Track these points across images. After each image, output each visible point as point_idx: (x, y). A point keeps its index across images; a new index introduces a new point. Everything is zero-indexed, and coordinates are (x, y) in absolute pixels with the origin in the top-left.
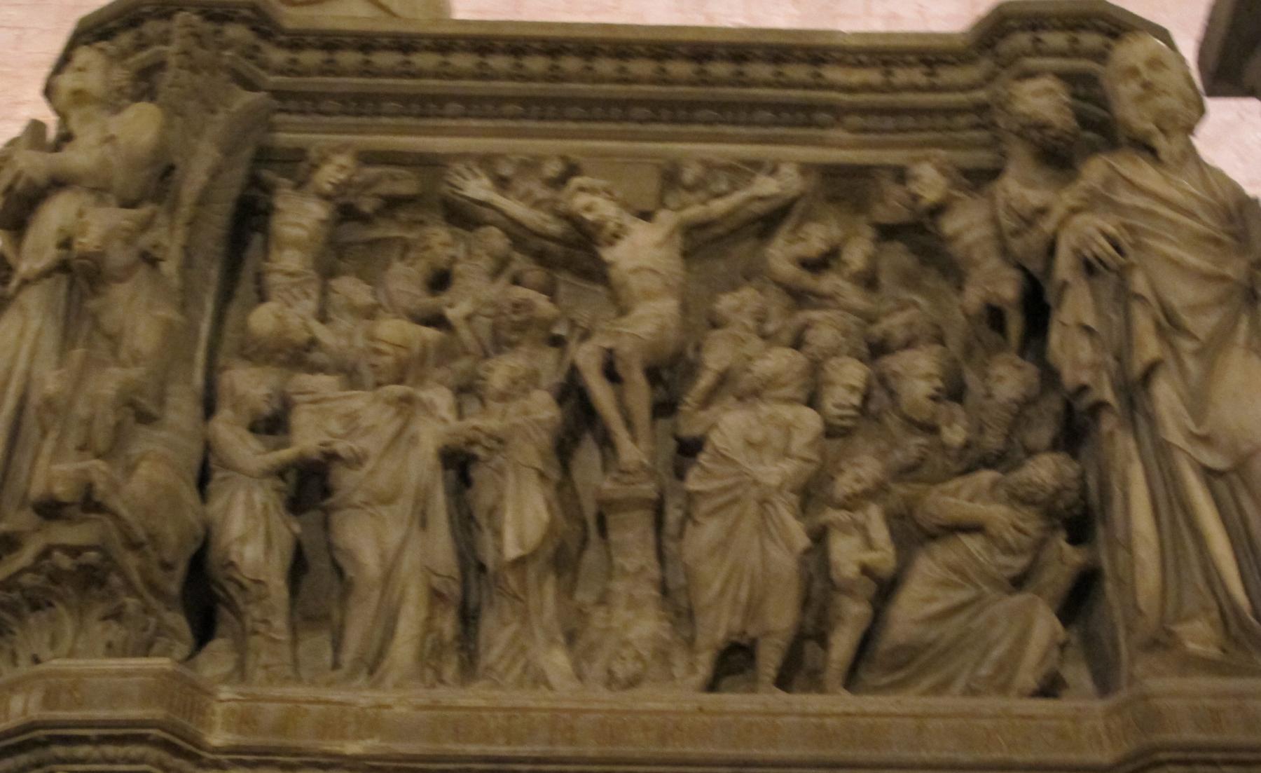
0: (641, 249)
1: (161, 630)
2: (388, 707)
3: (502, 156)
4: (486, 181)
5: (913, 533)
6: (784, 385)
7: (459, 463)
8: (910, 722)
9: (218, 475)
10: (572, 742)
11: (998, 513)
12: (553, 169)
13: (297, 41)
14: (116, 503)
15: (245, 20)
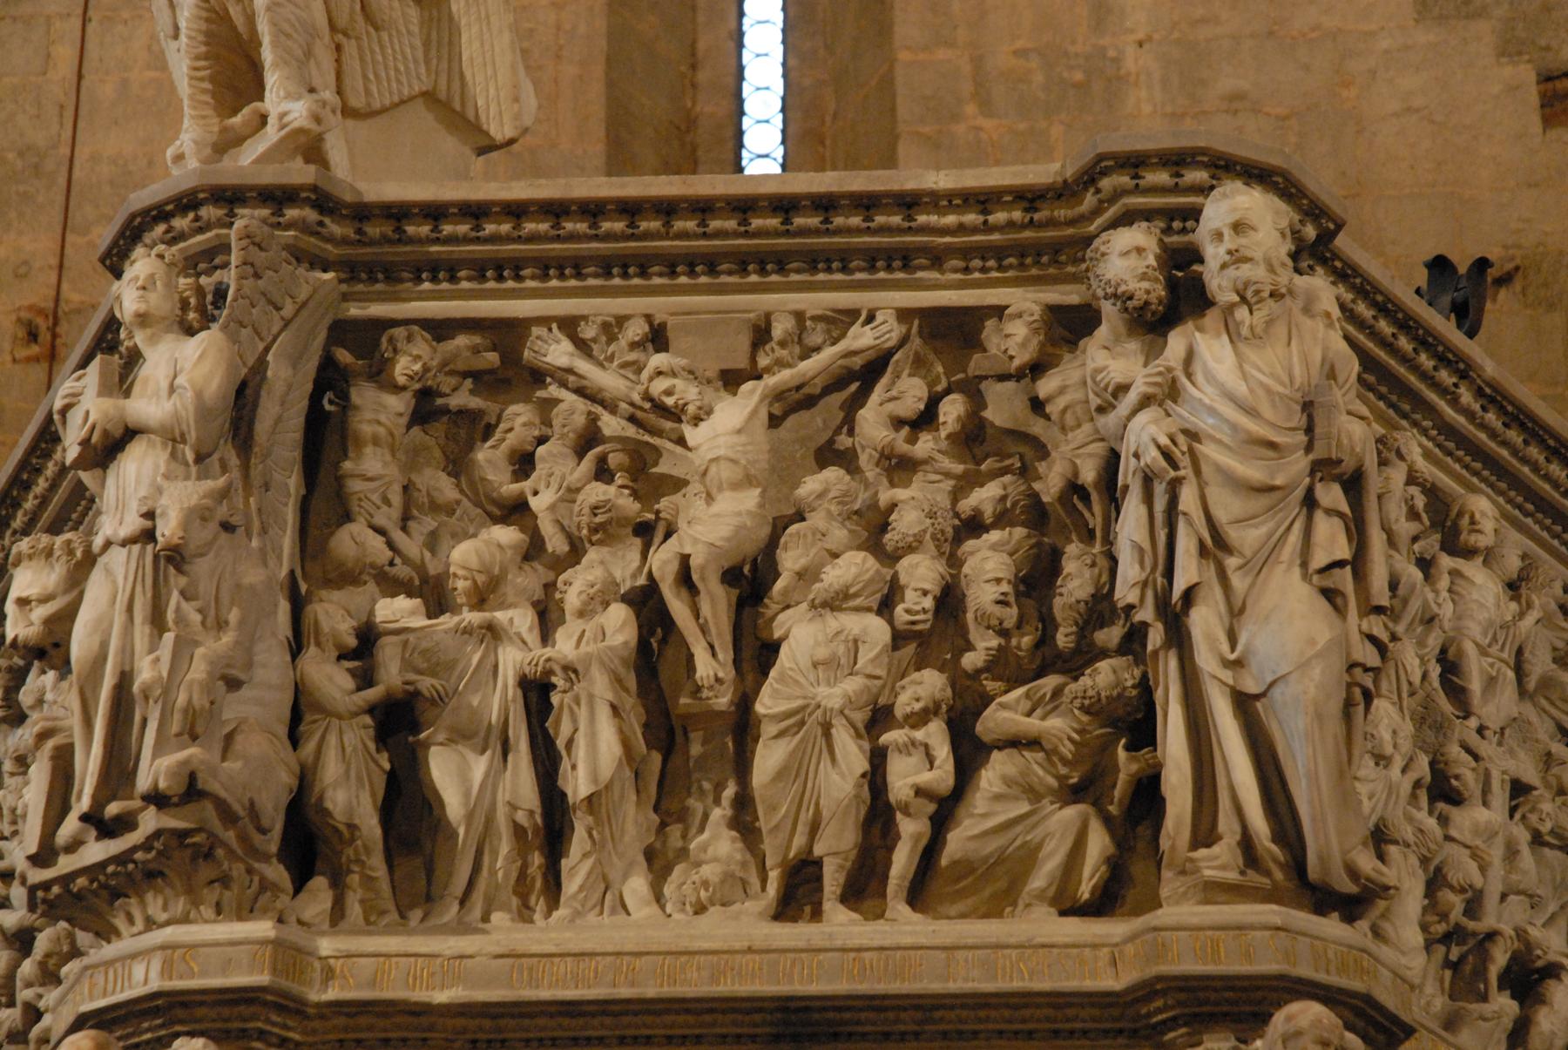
0: (725, 428)
1: (265, 886)
2: (471, 957)
3: (585, 318)
4: (566, 345)
5: (970, 753)
6: (856, 595)
7: (537, 693)
8: (942, 955)
9: (308, 717)
10: (633, 985)
11: (1057, 726)
12: (636, 330)
13: (362, 213)
14: (214, 787)
15: (307, 200)
